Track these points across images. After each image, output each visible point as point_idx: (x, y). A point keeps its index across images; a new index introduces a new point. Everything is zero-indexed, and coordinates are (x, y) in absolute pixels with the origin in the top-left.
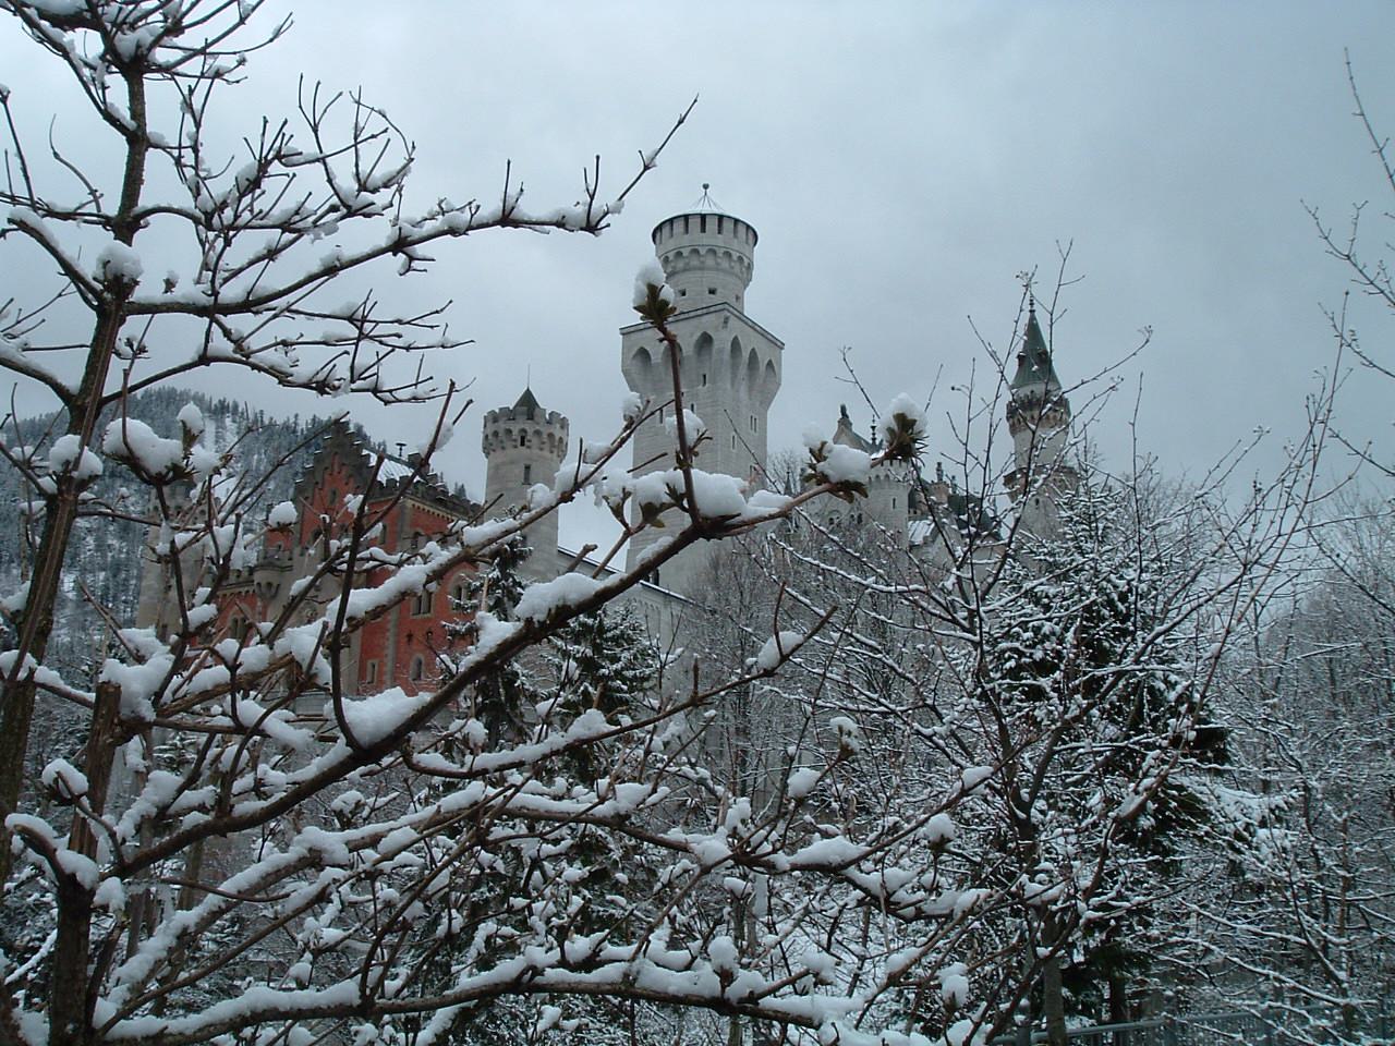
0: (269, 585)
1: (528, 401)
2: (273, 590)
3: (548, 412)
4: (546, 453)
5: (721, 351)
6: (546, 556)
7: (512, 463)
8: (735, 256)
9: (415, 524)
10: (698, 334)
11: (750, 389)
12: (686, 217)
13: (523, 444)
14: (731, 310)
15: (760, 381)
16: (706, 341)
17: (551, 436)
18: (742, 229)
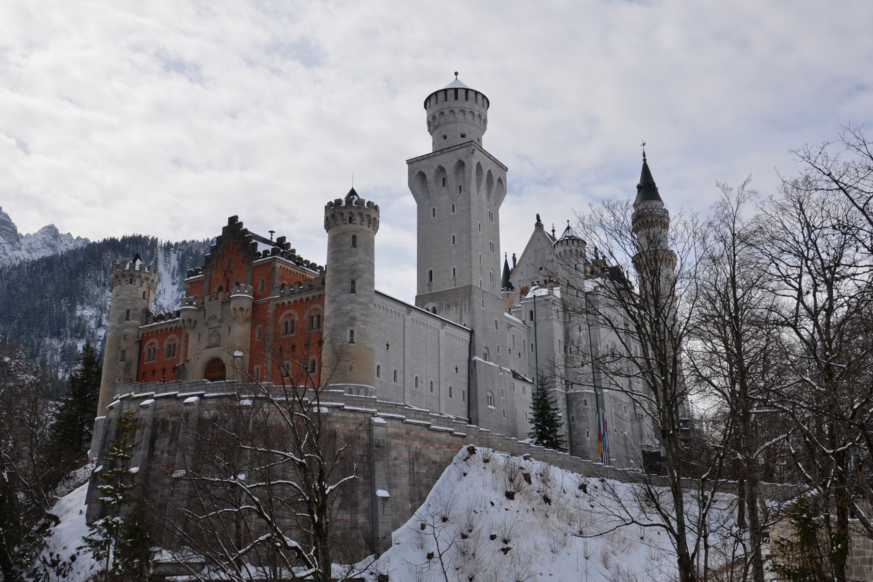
0: (190, 320)
1: (353, 192)
2: (192, 324)
3: (366, 201)
4: (365, 227)
5: (471, 171)
6: (367, 293)
7: (344, 234)
8: (476, 113)
9: (282, 278)
10: (456, 161)
11: (488, 196)
12: (445, 90)
13: (350, 222)
14: (474, 145)
15: (494, 190)
16: (461, 164)
17: (369, 216)
18: (480, 97)
